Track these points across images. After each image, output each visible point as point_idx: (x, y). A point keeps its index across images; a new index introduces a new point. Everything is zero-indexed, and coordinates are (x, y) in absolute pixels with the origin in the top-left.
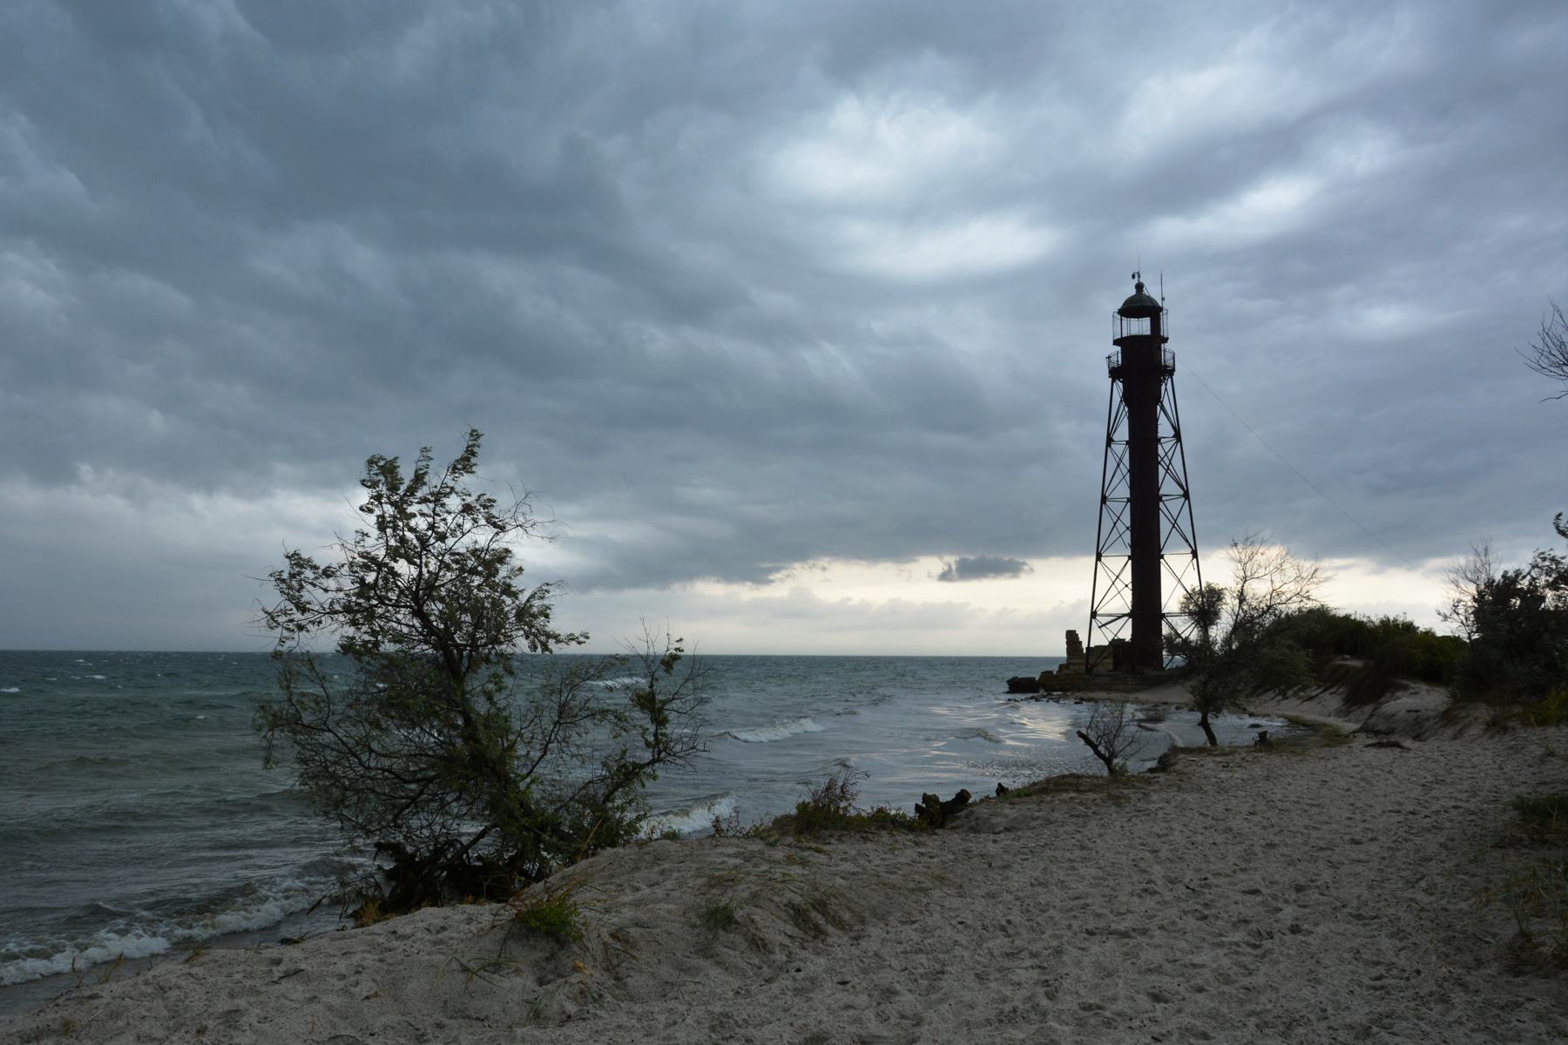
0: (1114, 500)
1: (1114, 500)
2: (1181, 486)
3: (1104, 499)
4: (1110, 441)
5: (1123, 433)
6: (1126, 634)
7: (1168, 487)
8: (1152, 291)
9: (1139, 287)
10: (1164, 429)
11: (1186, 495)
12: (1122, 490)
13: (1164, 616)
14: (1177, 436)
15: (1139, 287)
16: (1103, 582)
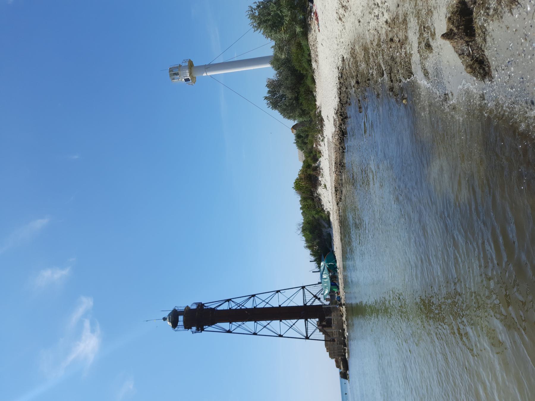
0: (256, 328)
1: (256, 328)
2: (251, 298)
3: (255, 334)
4: (229, 332)
5: (226, 325)
6: (315, 321)
7: (249, 305)
8: (166, 314)
9: (165, 319)
10: (225, 307)
11: (253, 296)
12: (250, 325)
13: (305, 305)
14: (228, 300)
15: (165, 319)
16: (291, 333)
